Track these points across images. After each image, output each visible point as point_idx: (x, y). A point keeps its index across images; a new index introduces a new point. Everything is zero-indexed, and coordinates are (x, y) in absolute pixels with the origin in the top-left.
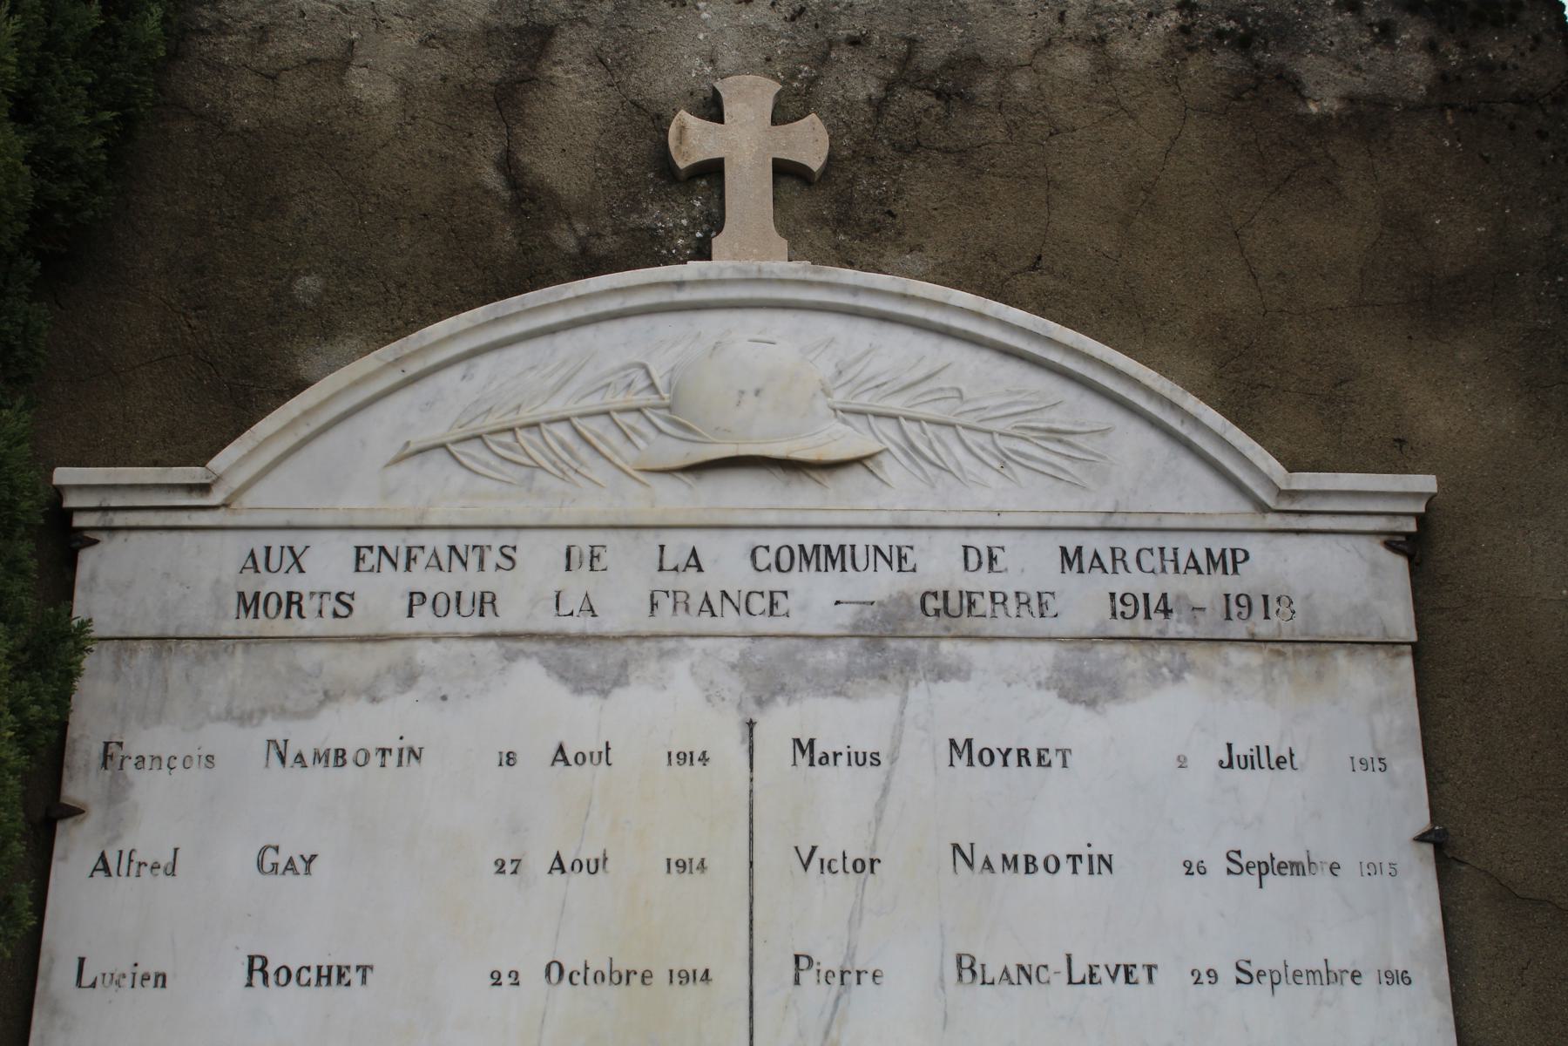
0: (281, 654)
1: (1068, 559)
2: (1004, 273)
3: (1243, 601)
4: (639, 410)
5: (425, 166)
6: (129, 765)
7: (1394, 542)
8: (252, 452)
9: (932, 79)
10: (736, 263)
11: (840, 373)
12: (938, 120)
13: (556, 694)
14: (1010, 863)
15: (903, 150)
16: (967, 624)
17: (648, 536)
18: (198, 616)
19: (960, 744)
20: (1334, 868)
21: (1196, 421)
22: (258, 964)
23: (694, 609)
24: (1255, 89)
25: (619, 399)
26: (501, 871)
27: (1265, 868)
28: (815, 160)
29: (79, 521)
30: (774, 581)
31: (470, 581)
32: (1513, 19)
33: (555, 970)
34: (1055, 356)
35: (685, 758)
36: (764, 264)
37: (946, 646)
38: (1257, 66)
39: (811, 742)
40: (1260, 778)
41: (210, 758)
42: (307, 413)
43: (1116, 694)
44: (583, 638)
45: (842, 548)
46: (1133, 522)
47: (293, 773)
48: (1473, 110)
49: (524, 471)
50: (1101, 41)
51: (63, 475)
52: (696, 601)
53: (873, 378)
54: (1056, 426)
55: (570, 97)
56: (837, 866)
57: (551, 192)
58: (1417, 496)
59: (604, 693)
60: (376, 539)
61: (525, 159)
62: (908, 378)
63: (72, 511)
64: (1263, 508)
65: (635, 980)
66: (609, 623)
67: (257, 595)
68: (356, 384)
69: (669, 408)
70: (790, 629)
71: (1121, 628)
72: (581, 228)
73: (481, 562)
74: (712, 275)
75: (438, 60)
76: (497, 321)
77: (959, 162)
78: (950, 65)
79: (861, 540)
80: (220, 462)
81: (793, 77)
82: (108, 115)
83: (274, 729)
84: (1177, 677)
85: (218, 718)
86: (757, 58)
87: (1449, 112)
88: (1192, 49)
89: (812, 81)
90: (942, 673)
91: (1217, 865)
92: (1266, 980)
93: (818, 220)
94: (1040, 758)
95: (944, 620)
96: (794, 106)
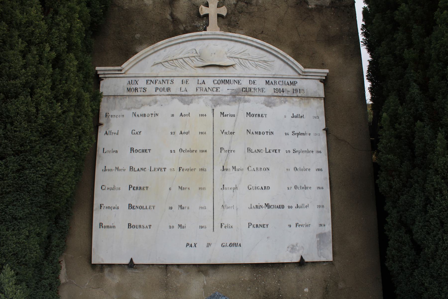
0: (134, 98)
1: (267, 82)
2: (257, 34)
3: (296, 90)
4: (194, 57)
5: (157, 15)
6: (110, 117)
7: (321, 81)
8: (129, 64)
10: (211, 31)
11: (229, 50)
12: (246, 7)
13: (181, 104)
14: (256, 133)
15: (240, 13)
16: (250, 93)
17: (196, 78)
18: (120, 92)
19: (248, 113)
20: (310, 134)
21: (289, 60)
22: (132, 149)
23: (204, 90)
24: (300, 3)
25: (190, 55)
26: (172, 134)
27: (298, 134)
28: (224, 14)
29: (100, 76)
30: (217, 86)
31: (166, 86)
33: (181, 150)
34: (265, 48)
35: (202, 115)
36: (216, 32)
37: (246, 97)
39: (223, 113)
40: (298, 119)
41: (123, 115)
42: (138, 57)
43: (274, 105)
44: (185, 95)
45: (229, 80)
46: (278, 76)
48: (337, 8)
49: (174, 67)
51: (97, 68)
52: (204, 89)
53: (234, 51)
54: (265, 60)
55: (182, 3)
56: (228, 133)
58: (325, 73)
59: (189, 105)
61: (175, 14)
62: (240, 51)
63: (99, 74)
64: (300, 75)
65: (194, 152)
66: (189, 93)
67: (130, 88)
68: (146, 52)
69: (199, 56)
70: (220, 94)
71: (276, 94)
72: (184, 26)
73: (168, 82)
74: (207, 34)
76: (170, 41)
77: (249, 15)
79: (232, 79)
80: (123, 66)
82: (103, 6)
83: (134, 111)
84: (285, 102)
85: (124, 109)
87: (333, 8)
90: (245, 101)
91: (291, 133)
92: (298, 152)
93: (226, 25)
94: (262, 116)
95: (246, 92)
96: (221, 5)
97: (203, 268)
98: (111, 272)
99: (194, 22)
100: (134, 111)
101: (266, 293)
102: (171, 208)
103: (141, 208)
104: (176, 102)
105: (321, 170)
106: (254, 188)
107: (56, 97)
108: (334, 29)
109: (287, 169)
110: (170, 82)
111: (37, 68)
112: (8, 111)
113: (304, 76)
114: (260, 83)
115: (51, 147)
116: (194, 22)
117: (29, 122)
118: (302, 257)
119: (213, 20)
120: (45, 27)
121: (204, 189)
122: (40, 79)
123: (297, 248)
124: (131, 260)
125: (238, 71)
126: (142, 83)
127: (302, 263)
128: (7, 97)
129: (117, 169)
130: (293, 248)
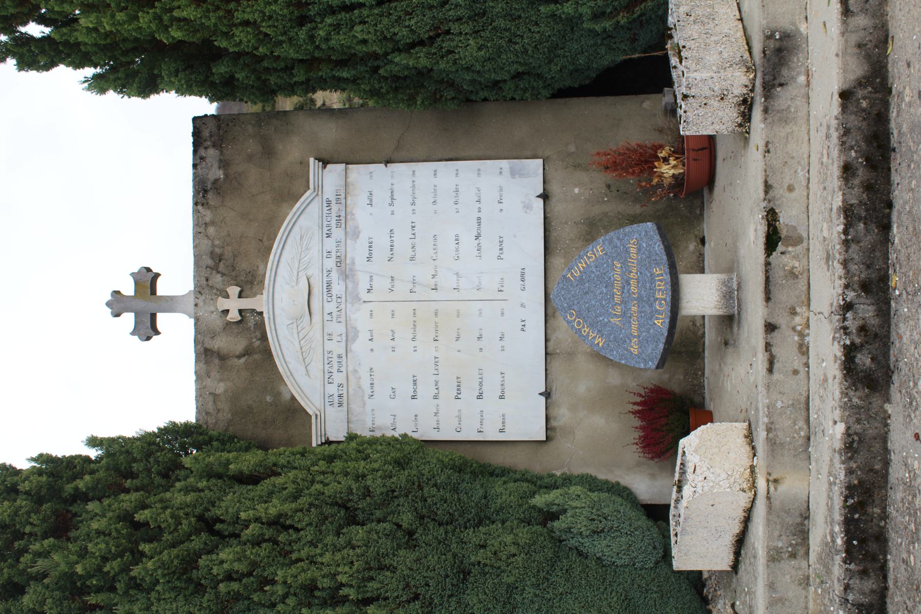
0: (351, 397)
14: (392, 250)
15: (234, 269)
16: (343, 258)
25: (295, 331)
27: (392, 199)
29: (324, 441)
30: (334, 297)
31: (335, 360)
32: (198, 129)
34: (284, 238)
35: (371, 315)
37: (348, 262)
42: (300, 395)
43: (357, 227)
44: (347, 336)
47: (375, 393)
49: (312, 351)
50: (206, 224)
51: (314, 445)
52: (339, 313)
58: (314, 162)
61: (238, 353)
64: (317, 194)
66: (344, 331)
68: (293, 386)
71: (343, 226)
72: (254, 340)
75: (214, 374)
78: (212, 259)
79: (325, 279)
83: (366, 397)
86: (212, 302)
88: (208, 203)
89: (217, 290)
90: (353, 263)
93: (251, 288)
96: (224, 294)
97: (550, 312)
98: (555, 418)
99: (249, 328)
100: (366, 397)
101: (580, 238)
102: (481, 349)
103: (481, 384)
104: (355, 347)
105: (435, 171)
106: (457, 253)
107: (365, 459)
108: (252, 146)
110: (330, 355)
111: (337, 474)
112: (382, 494)
113: (319, 189)
114: (330, 244)
115: (413, 463)
116: (249, 328)
117: (391, 477)
118: (538, 196)
119: (246, 304)
120: (294, 472)
121: (458, 311)
122: (349, 470)
123: (527, 201)
124: (540, 394)
125: (314, 272)
126: (332, 389)
127: (545, 196)
128: (369, 496)
129: (436, 414)
130: (527, 207)
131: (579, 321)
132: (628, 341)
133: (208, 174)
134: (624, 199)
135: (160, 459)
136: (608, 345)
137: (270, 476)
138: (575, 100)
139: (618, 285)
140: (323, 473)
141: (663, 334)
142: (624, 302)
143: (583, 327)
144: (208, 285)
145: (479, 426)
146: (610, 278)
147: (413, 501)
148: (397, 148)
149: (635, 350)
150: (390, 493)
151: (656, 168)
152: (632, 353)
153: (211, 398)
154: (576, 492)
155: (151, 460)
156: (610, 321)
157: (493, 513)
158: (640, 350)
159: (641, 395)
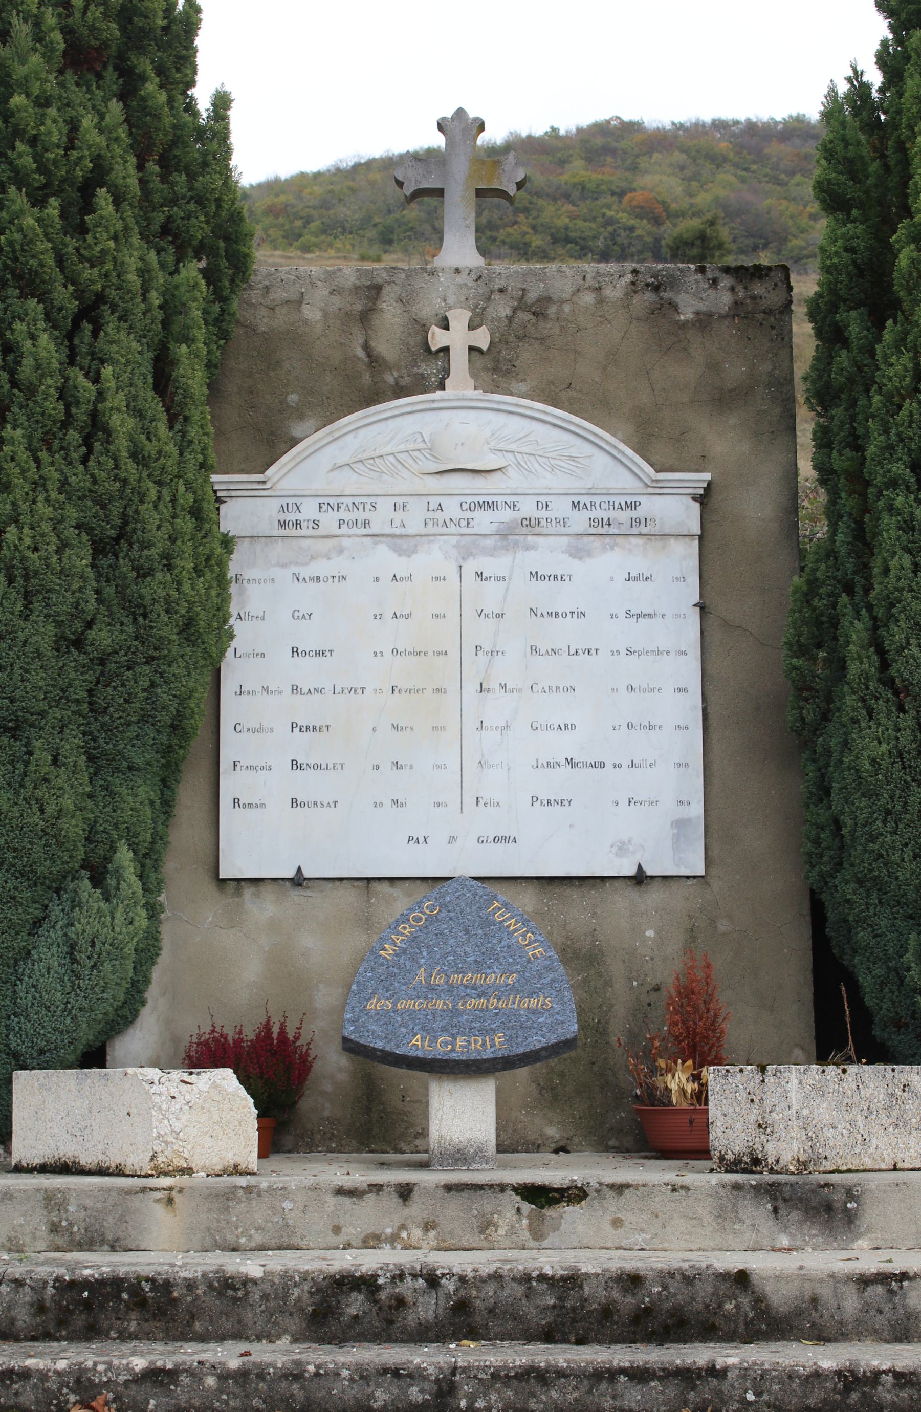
1: (575, 505)
6: (245, 582)
9: (531, 307)
14: (550, 614)
15: (519, 338)
16: (538, 530)
17: (423, 498)
18: (265, 528)
20: (663, 616)
23: (440, 525)
25: (411, 446)
26: (375, 618)
27: (638, 616)
29: (219, 494)
30: (469, 514)
31: (361, 515)
32: (767, 275)
34: (572, 428)
35: (438, 579)
37: (529, 538)
38: (661, 299)
42: (299, 453)
43: (589, 554)
44: (401, 536)
46: (598, 492)
47: (302, 585)
48: (746, 318)
50: (599, 289)
51: (214, 478)
52: (441, 522)
56: (490, 616)
57: (383, 358)
59: (409, 556)
60: (326, 500)
61: (373, 344)
64: (649, 486)
65: (422, 654)
66: (410, 531)
68: (316, 442)
71: (593, 531)
72: (396, 374)
74: (446, 397)
75: (337, 302)
77: (541, 344)
78: (539, 300)
79: (501, 499)
81: (477, 307)
84: (612, 549)
86: (463, 299)
88: (635, 292)
89: (484, 309)
90: (528, 548)
93: (486, 369)
95: (529, 528)
98: (257, 895)
103: (318, 767)
104: (383, 550)
105: (686, 690)
106: (544, 727)
109: (613, 690)
110: (368, 507)
111: (172, 524)
112: (141, 597)
113: (657, 489)
115: (188, 649)
117: (167, 612)
118: (640, 866)
119: (459, 360)
120: (175, 452)
121: (443, 728)
122: (179, 543)
124: (299, 869)
125: (514, 480)
126: (309, 510)
127: (640, 879)
128: (137, 577)
129: (266, 690)
130: (622, 848)
131: (421, 919)
132: (388, 994)
133: (686, 292)
134: (635, 1016)
135: (193, 220)
136: (382, 965)
137: (168, 411)
138: (806, 932)
139: (479, 979)
140: (174, 501)
141: (398, 1047)
142: (451, 988)
143: (411, 926)
144: (492, 292)
145: (244, 763)
146: (489, 968)
147: (129, 648)
148: (727, 625)
149: (373, 1005)
150: (142, 611)
151: (684, 1062)
152: (368, 1001)
153: (295, 296)
154: (137, 918)
155: (192, 206)
156: (420, 967)
157: (105, 780)
158: (373, 1013)
159: (297, 1039)
